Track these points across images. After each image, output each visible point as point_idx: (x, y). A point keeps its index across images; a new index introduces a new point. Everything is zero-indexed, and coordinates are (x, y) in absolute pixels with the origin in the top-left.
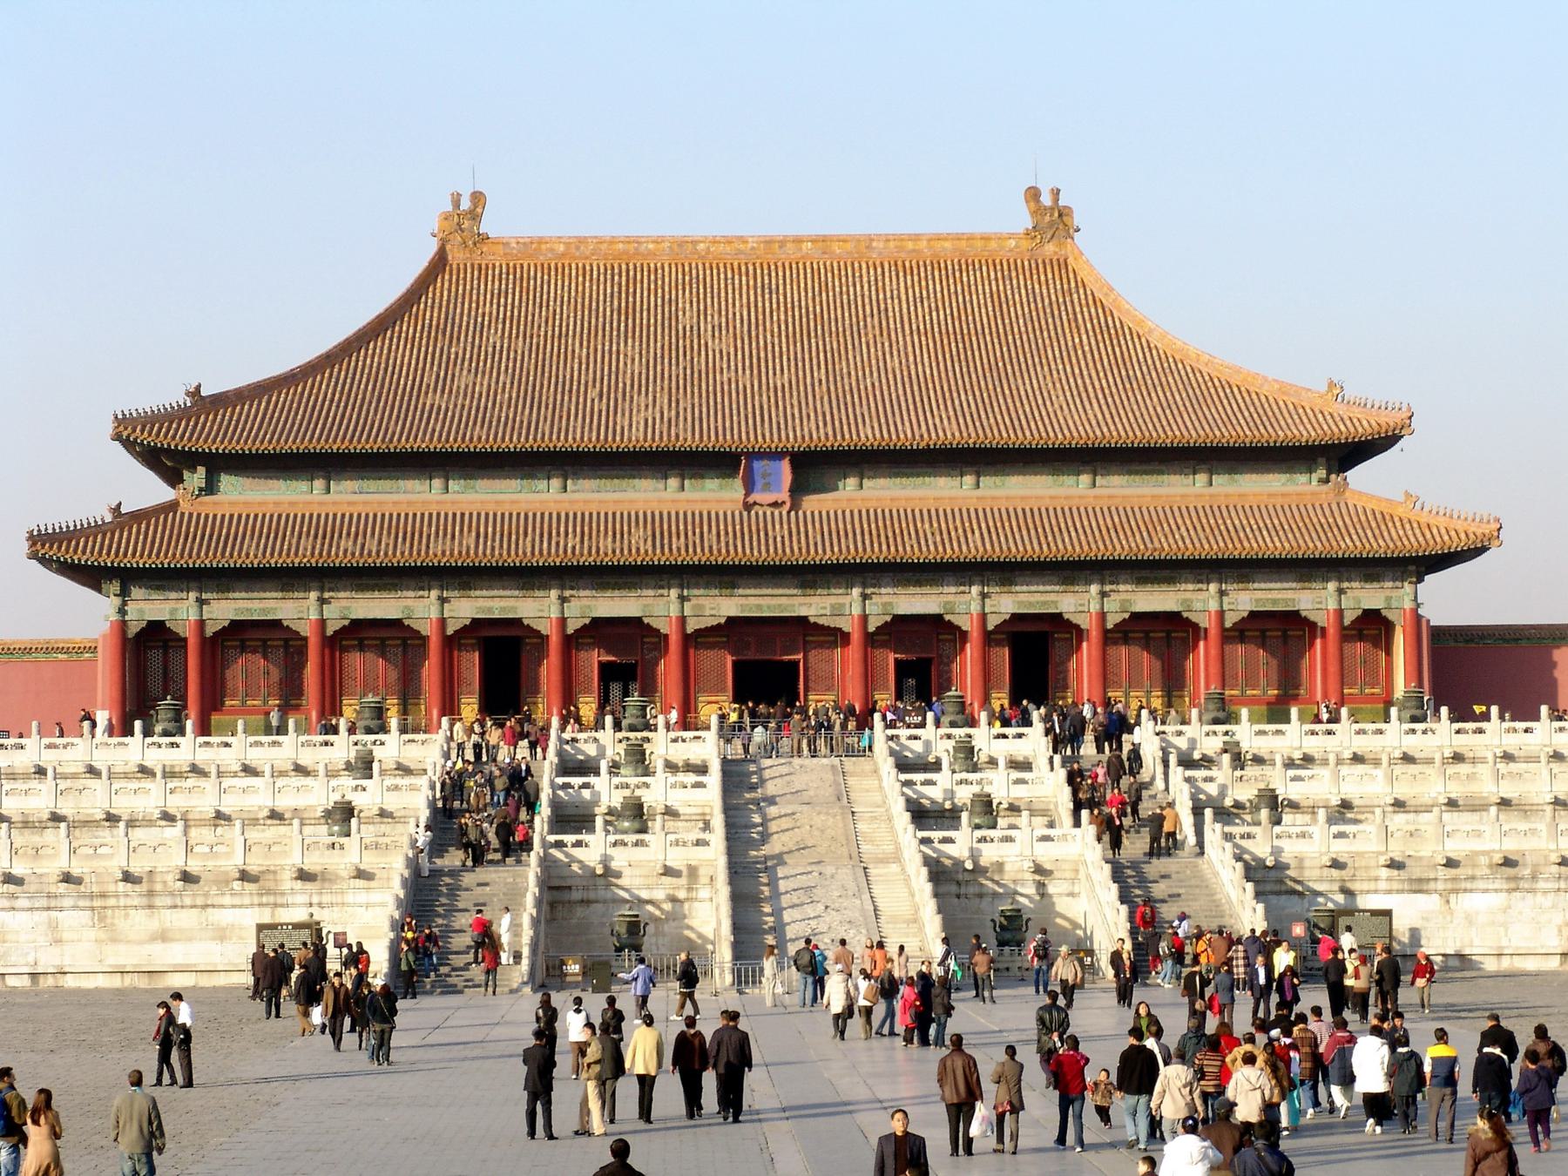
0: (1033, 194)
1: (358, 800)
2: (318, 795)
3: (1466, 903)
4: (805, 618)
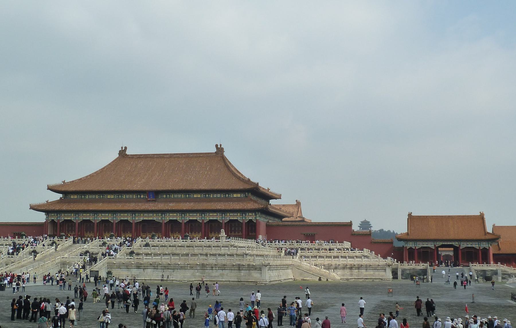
3: (146, 270)
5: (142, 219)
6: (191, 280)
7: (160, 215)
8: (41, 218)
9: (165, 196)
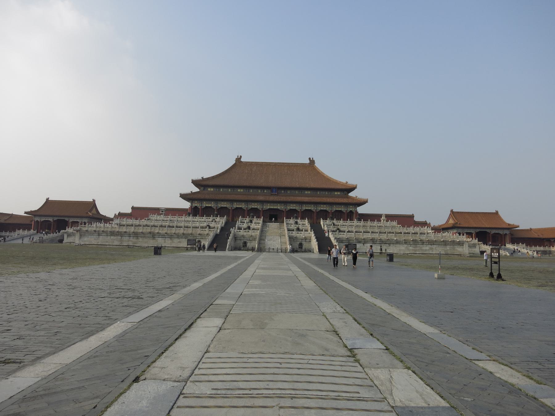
1: (211, 225)
2: (205, 224)
5: (268, 207)
6: (406, 253)
8: (186, 205)
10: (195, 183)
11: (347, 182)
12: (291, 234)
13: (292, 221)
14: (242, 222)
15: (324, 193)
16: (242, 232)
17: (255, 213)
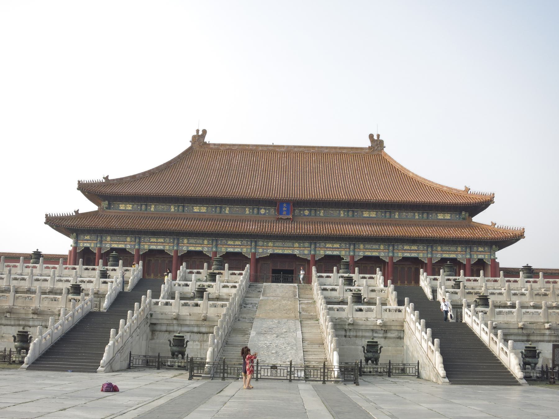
0: (371, 136)
4: (295, 255)
5: (270, 251)
7: (307, 245)
9: (307, 212)
10: (88, 189)
11: (467, 189)
12: (338, 315)
13: (335, 279)
14: (183, 280)
15: (410, 215)
16: (175, 308)
17: (235, 261)
